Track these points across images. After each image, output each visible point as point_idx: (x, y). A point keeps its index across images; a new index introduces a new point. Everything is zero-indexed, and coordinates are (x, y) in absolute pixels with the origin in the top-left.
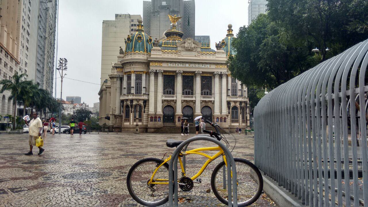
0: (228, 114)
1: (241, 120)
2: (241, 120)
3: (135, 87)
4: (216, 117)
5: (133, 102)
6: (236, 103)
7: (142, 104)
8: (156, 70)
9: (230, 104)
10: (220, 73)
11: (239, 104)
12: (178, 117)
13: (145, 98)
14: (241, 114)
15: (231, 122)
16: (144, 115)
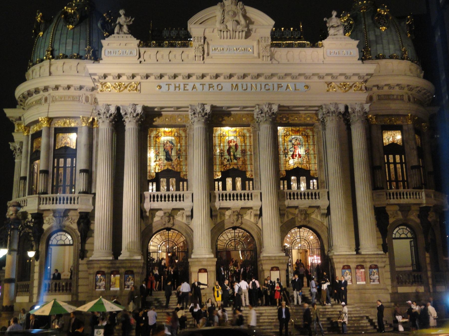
0: (382, 252)
1: (429, 274)
2: (429, 274)
3: (51, 170)
4: (341, 266)
5: (42, 223)
6: (409, 211)
7: (75, 226)
8: (118, 109)
9: (387, 217)
10: (342, 109)
11: (419, 216)
12: (197, 269)
13: (83, 205)
14: (427, 250)
15: (395, 283)
16: (81, 268)
